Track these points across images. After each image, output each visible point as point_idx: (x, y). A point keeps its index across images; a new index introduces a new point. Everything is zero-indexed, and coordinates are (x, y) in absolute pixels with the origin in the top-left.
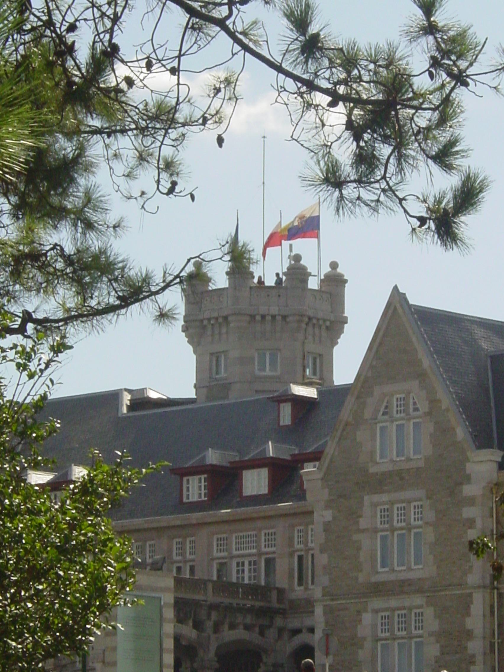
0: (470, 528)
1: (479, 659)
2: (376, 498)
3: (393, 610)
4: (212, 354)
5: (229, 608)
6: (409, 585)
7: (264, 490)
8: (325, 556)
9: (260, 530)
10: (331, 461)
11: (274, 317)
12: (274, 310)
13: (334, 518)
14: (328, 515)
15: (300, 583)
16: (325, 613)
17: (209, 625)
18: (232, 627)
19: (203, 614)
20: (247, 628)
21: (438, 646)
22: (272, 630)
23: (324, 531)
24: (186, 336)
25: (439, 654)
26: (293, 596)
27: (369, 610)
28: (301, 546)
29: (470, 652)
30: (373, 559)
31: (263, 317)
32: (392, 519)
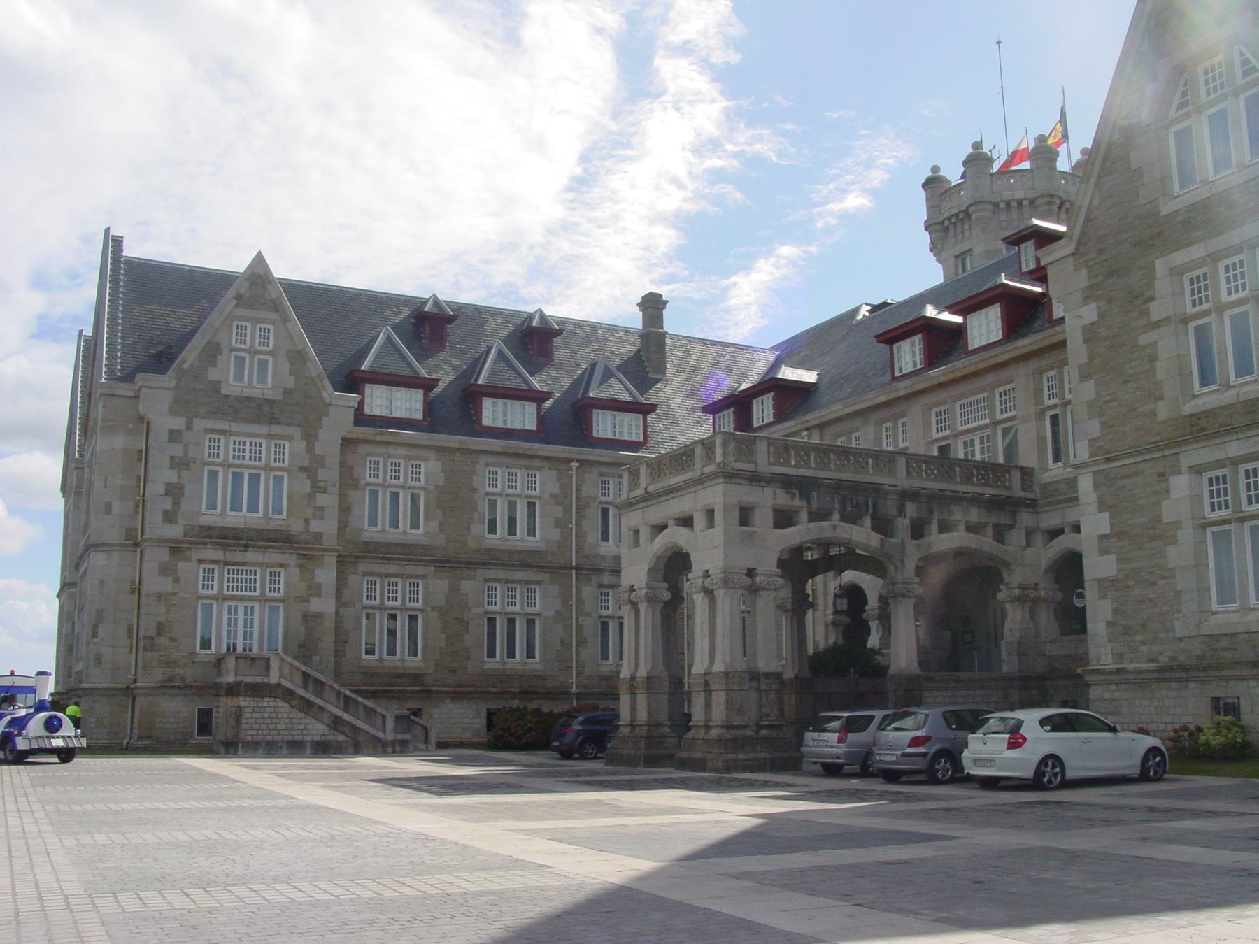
2: (1179, 258)
3: (1235, 462)
4: (957, 257)
5: (936, 499)
7: (996, 334)
8: (1090, 386)
9: (993, 388)
10: (1088, 220)
11: (1020, 203)
12: (1019, 194)
13: (1101, 316)
15: (1057, 458)
16: (1096, 486)
17: (903, 524)
18: (944, 528)
19: (890, 508)
20: (970, 528)
22: (1014, 532)
23: (1085, 341)
24: (934, 255)
26: (1046, 477)
27: (1184, 468)
28: (1055, 401)
30: (1184, 373)
31: (1008, 204)
32: (1217, 291)
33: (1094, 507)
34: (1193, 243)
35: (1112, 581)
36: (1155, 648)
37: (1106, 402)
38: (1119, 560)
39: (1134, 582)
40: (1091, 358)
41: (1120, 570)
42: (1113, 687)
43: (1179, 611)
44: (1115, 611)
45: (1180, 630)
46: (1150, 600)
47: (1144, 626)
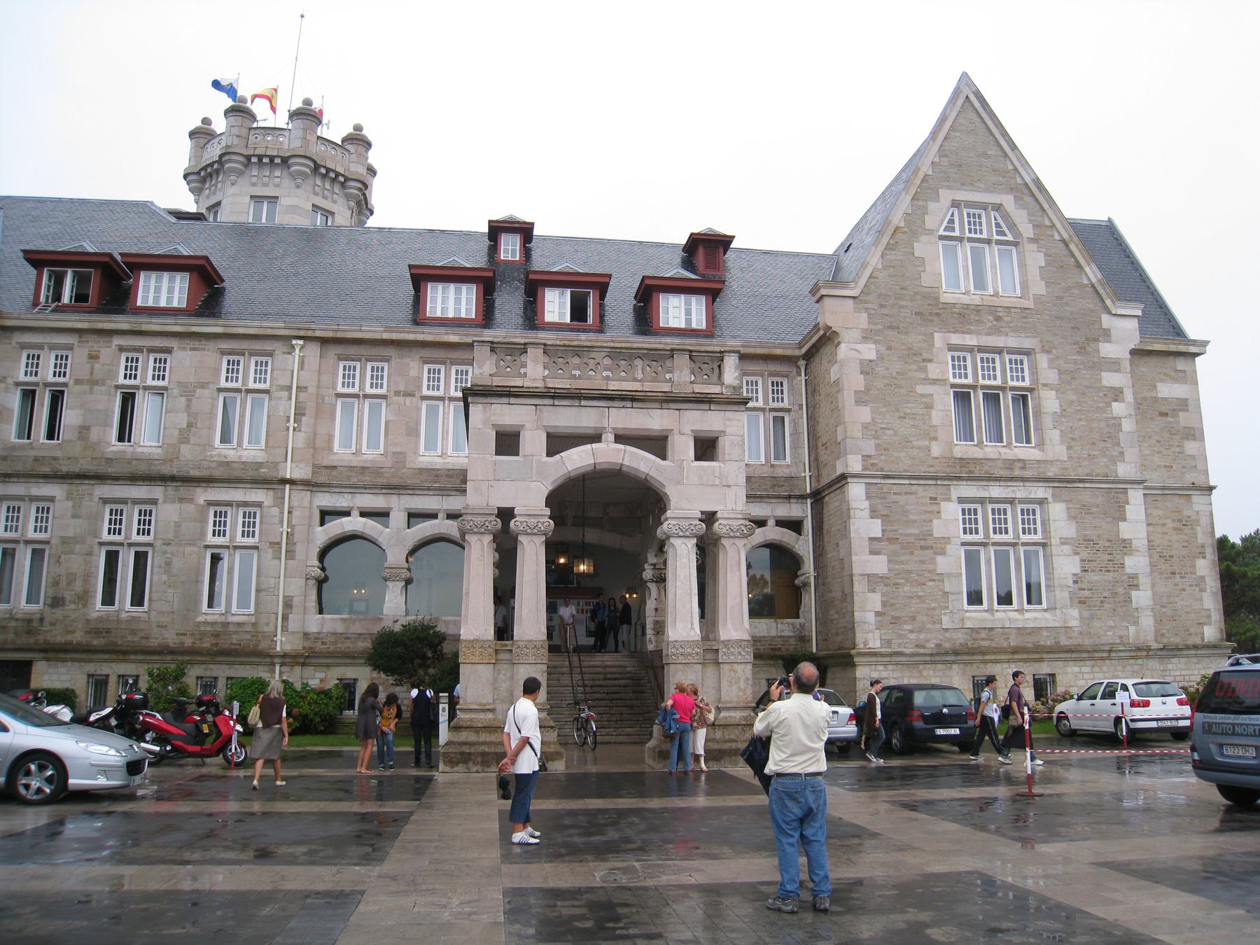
0: (1116, 400)
1: (1144, 581)
2: (956, 339)
6: (1023, 468)
13: (880, 358)
14: (869, 351)
16: (868, 497)
21: (1077, 558)
25: (1078, 571)
27: (954, 496)
29: (1128, 570)
33: (866, 513)
34: (968, 333)
35: (882, 577)
36: (922, 636)
37: (882, 428)
38: (889, 561)
39: (903, 581)
40: (868, 389)
41: (890, 570)
42: (881, 668)
43: (947, 608)
44: (884, 604)
45: (946, 622)
46: (920, 597)
47: (914, 618)
